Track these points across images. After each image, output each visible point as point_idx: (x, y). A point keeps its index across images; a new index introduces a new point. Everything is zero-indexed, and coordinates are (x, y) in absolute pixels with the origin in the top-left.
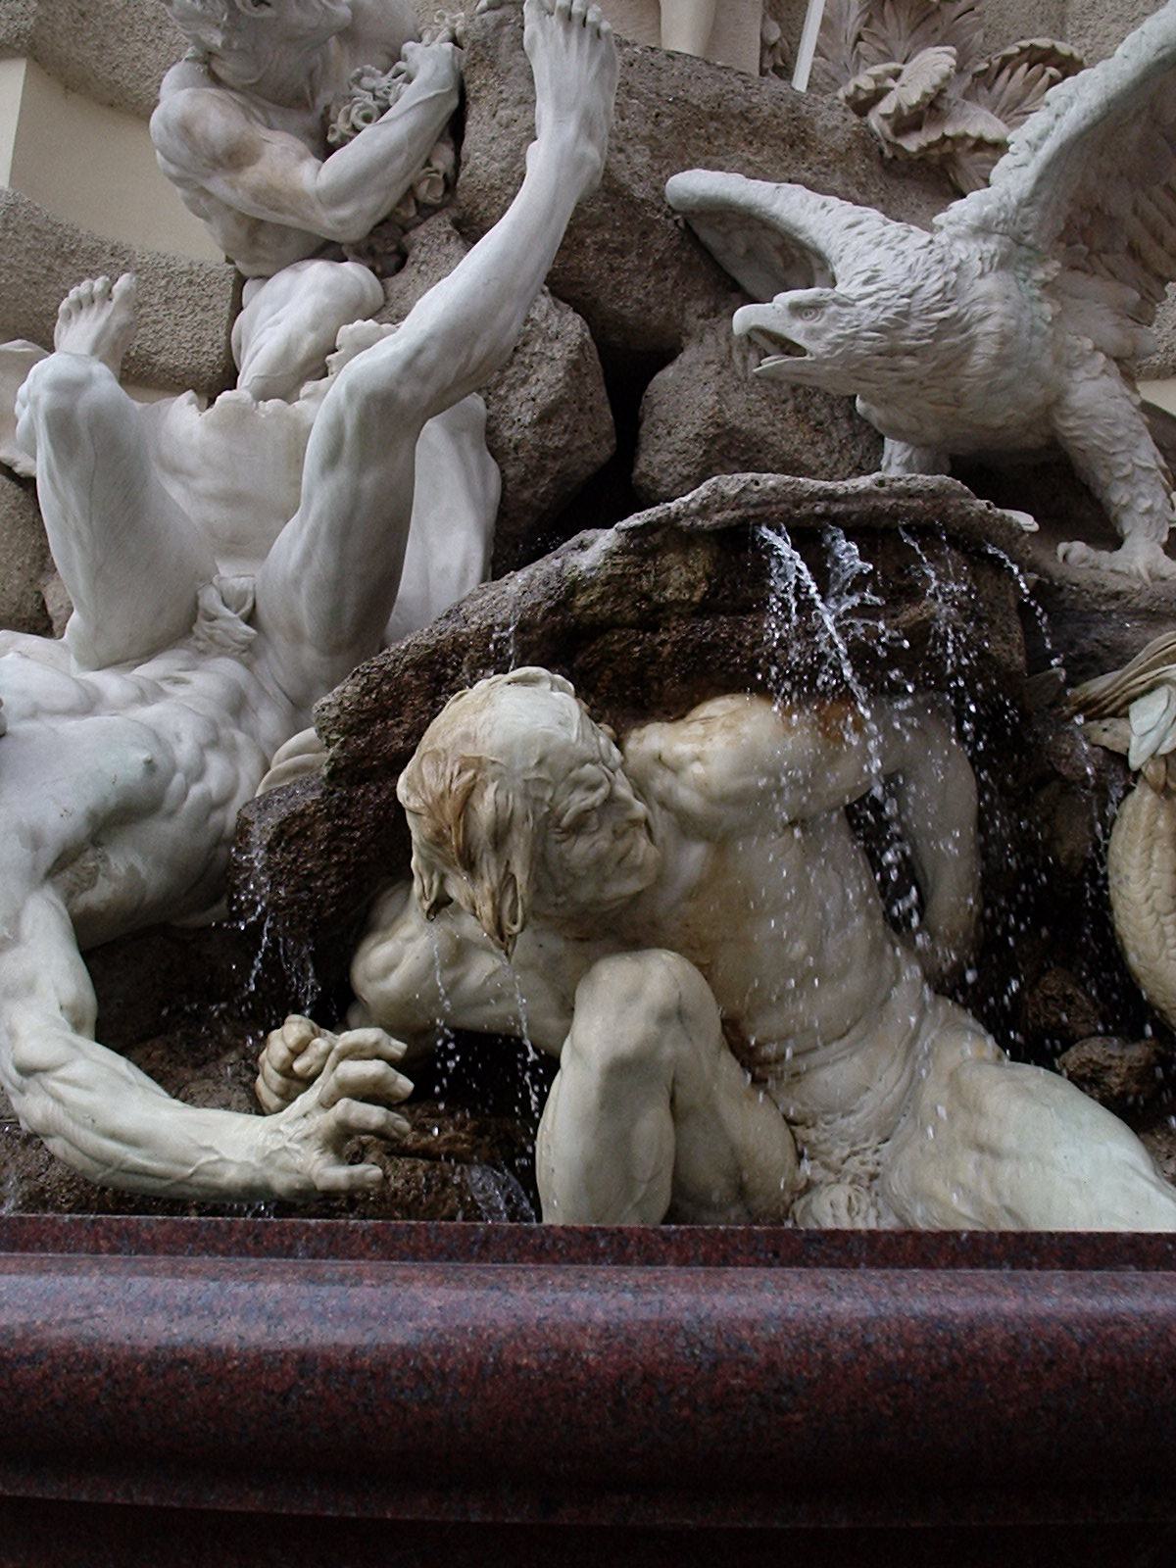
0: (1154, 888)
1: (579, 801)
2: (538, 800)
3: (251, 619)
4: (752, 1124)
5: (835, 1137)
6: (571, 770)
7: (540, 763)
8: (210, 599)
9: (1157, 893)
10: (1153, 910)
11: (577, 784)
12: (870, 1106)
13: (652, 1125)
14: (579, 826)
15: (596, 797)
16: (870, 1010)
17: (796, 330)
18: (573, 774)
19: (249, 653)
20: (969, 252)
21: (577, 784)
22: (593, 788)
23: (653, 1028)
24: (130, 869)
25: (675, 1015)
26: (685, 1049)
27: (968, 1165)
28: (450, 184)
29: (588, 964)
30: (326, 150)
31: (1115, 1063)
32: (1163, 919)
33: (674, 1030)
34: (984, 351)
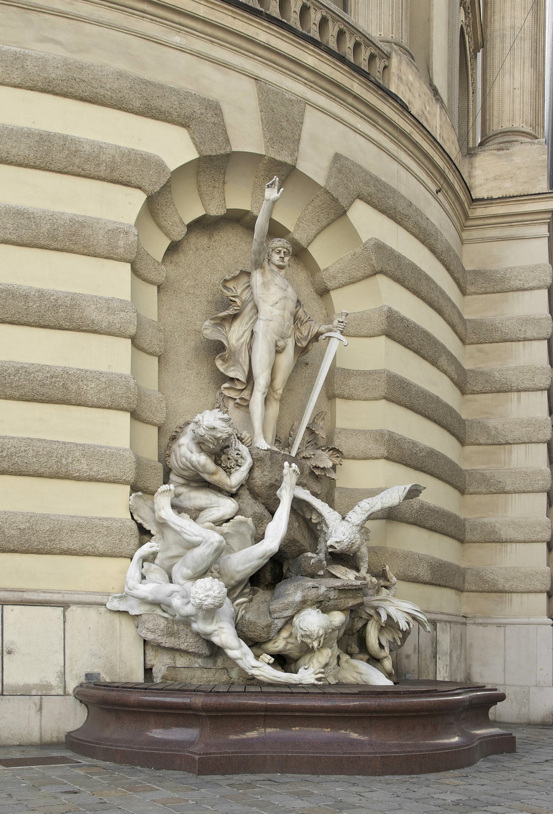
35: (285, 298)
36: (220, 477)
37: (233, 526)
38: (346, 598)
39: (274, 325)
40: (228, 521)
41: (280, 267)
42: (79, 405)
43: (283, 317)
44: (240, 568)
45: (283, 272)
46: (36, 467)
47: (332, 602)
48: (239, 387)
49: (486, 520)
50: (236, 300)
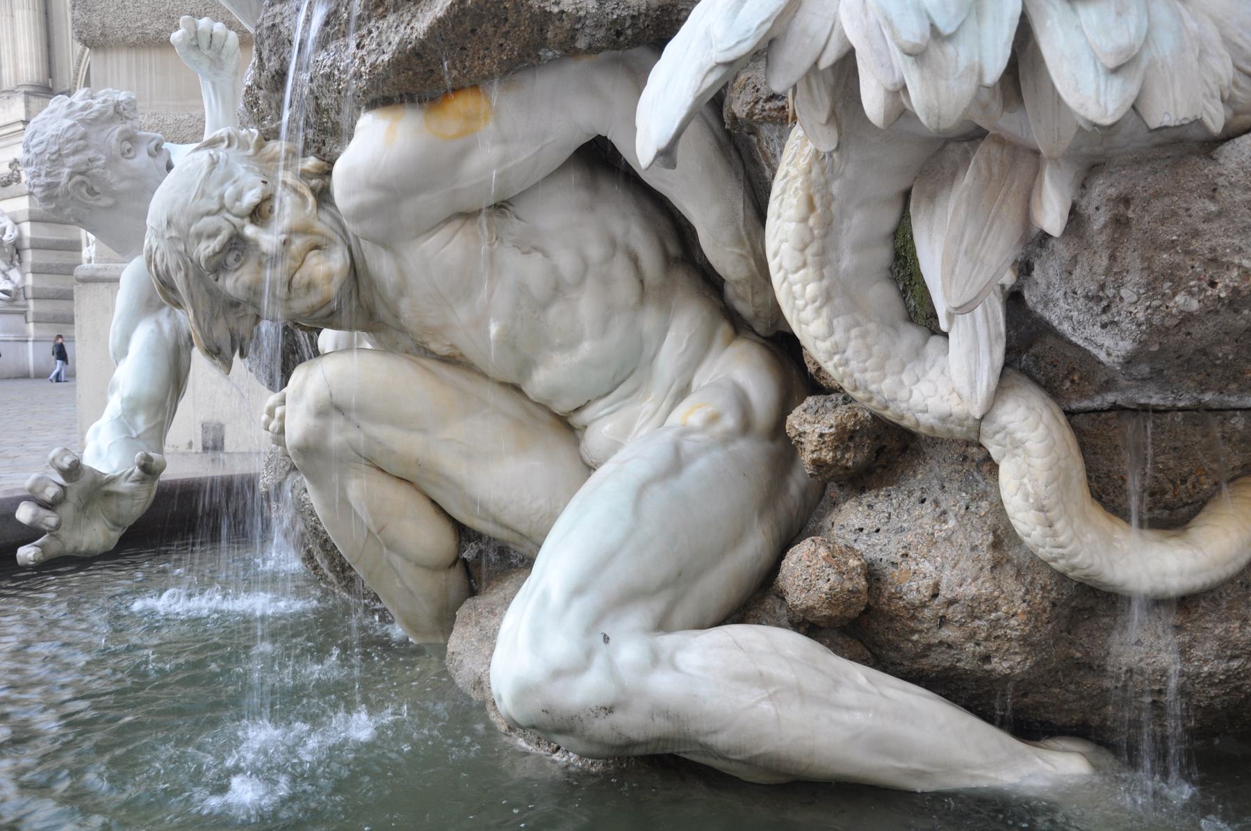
0: (782, 241)
1: (205, 249)
2: (180, 252)
6: (190, 225)
7: (169, 223)
9: (785, 246)
10: (780, 267)
11: (199, 236)
14: (218, 265)
15: (215, 244)
18: (192, 230)
21: (199, 236)
22: (212, 236)
23: (311, 421)
26: (352, 434)
31: (808, 428)
32: (792, 277)
33: (337, 421)
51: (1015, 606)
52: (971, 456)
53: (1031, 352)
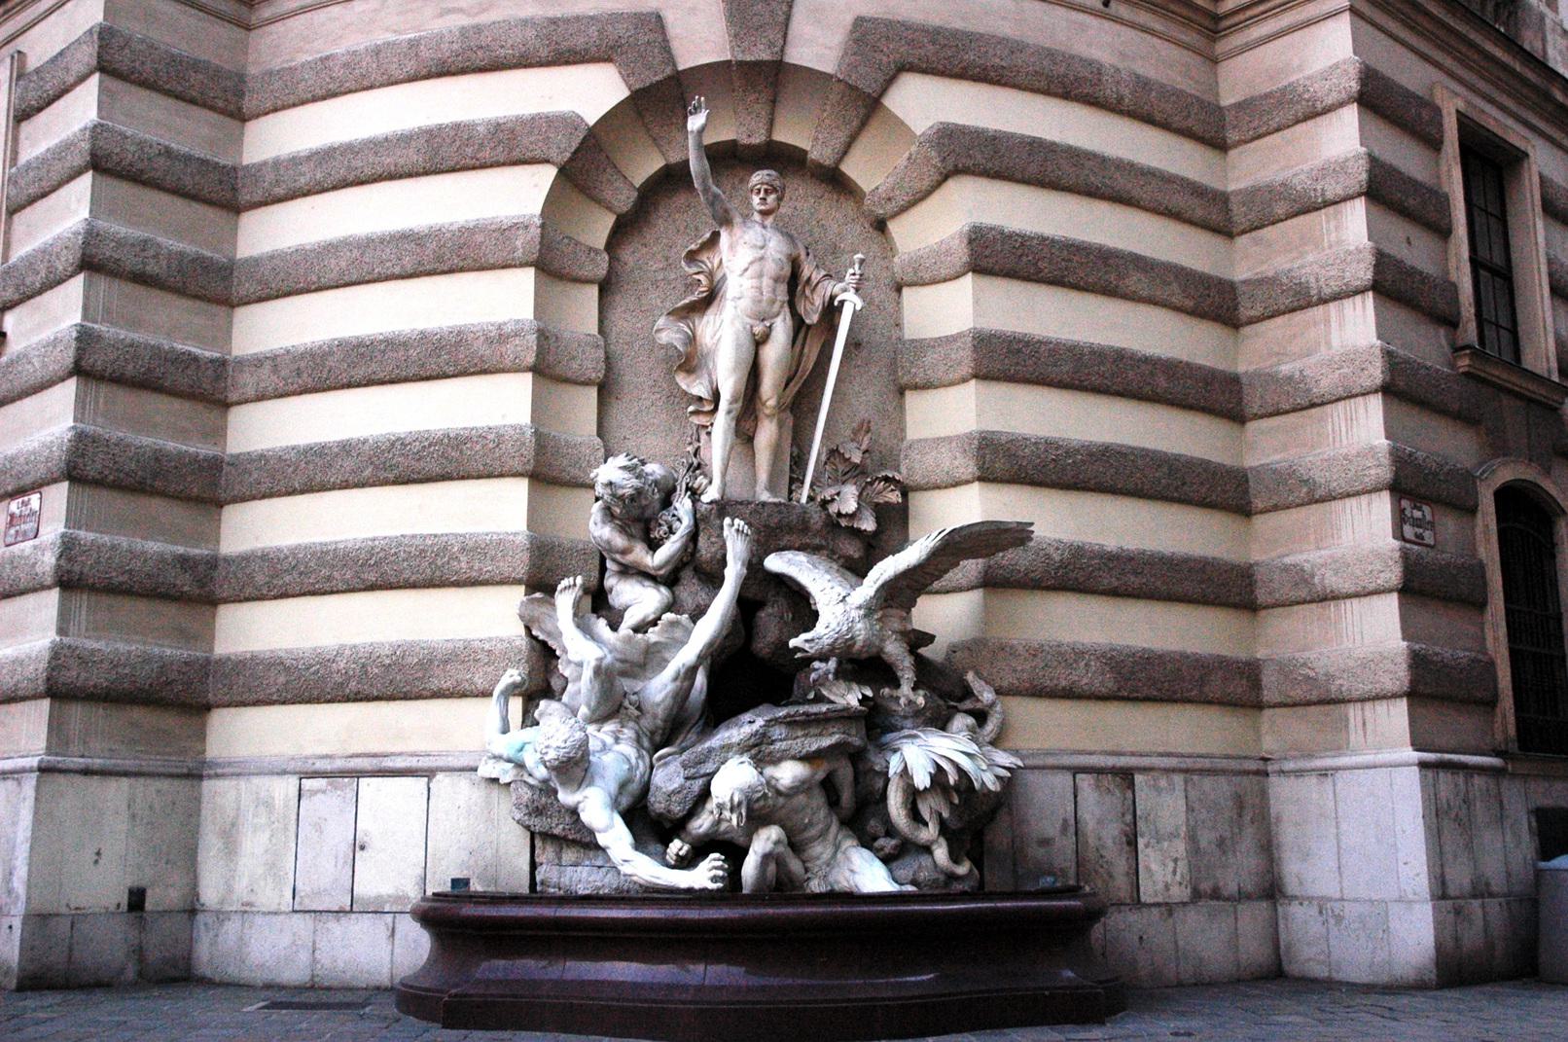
3: (639, 708)
4: (795, 865)
5: (814, 866)
8: (626, 703)
12: (826, 856)
13: (772, 868)
16: (823, 834)
17: (807, 647)
19: (637, 720)
20: (855, 614)
24: (625, 801)
25: (777, 843)
27: (847, 874)
28: (693, 554)
29: (756, 830)
30: (653, 545)
34: (858, 646)
35: (762, 258)
36: (640, 555)
37: (663, 631)
38: (806, 736)
39: (745, 303)
40: (654, 623)
41: (765, 213)
42: (463, 478)
43: (759, 289)
44: (659, 698)
45: (769, 221)
46: (406, 574)
47: (778, 745)
48: (708, 408)
49: (1287, 560)
50: (701, 277)
51: (942, 877)
52: (927, 849)
53: (944, 829)
